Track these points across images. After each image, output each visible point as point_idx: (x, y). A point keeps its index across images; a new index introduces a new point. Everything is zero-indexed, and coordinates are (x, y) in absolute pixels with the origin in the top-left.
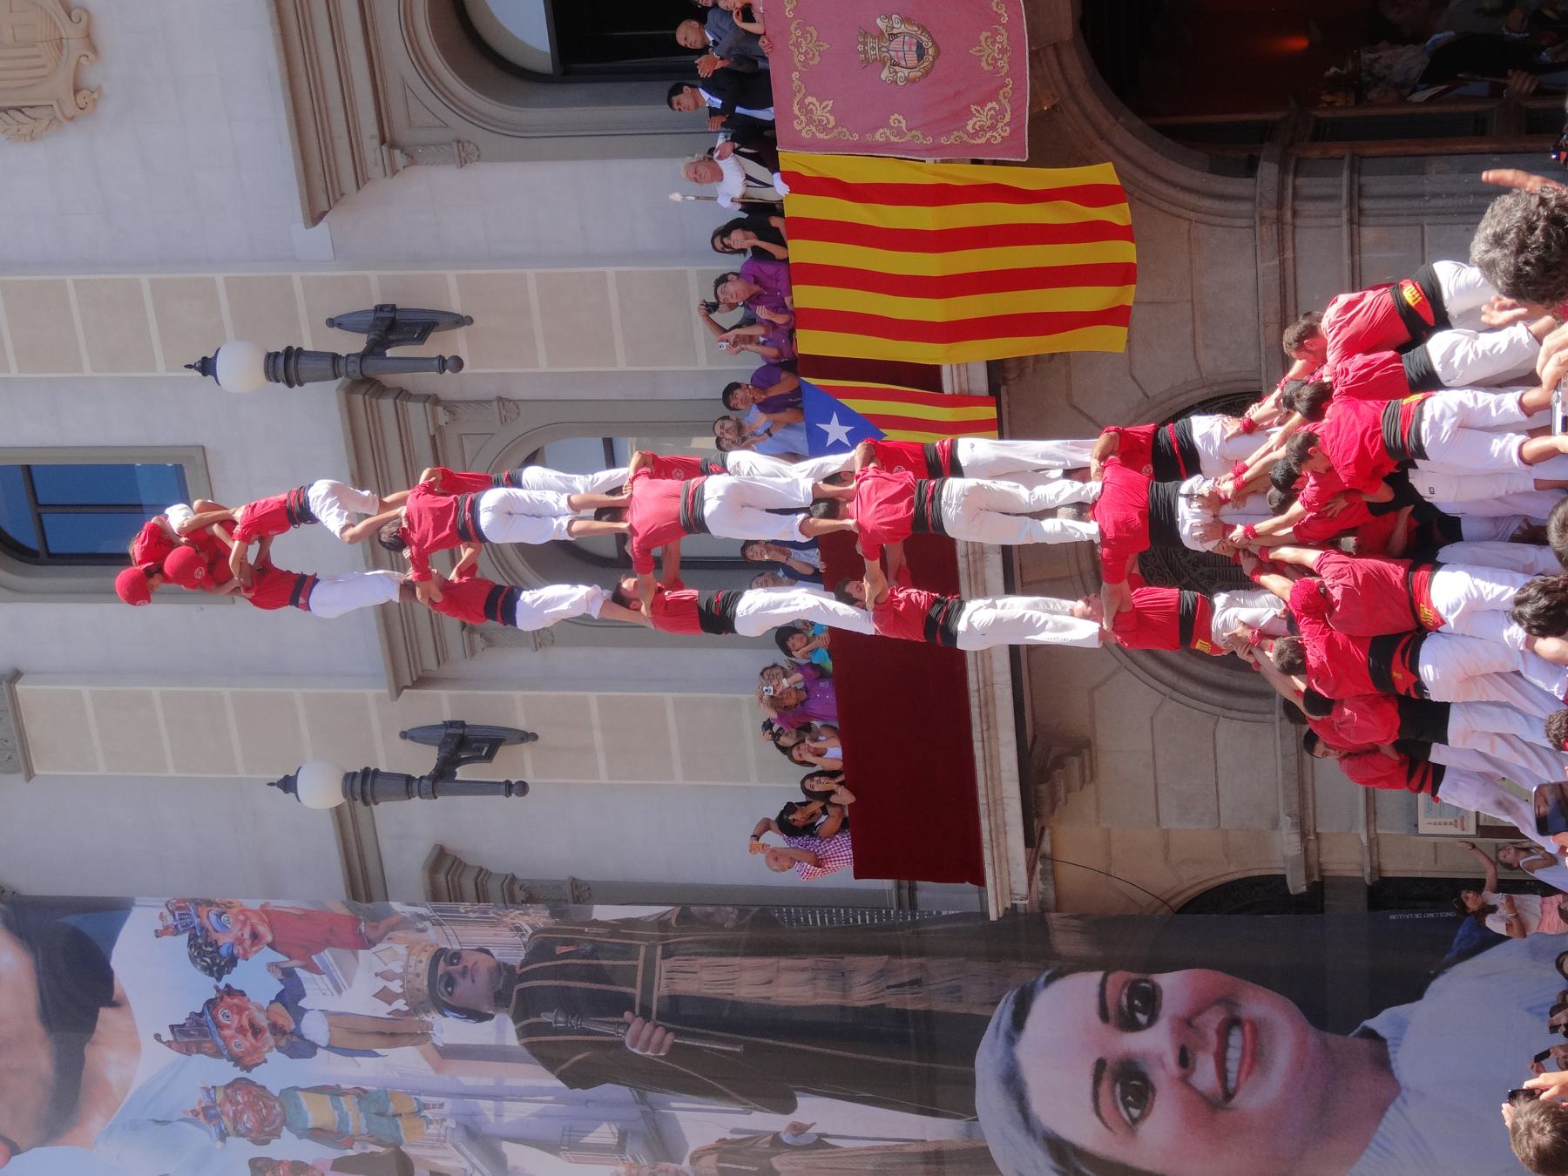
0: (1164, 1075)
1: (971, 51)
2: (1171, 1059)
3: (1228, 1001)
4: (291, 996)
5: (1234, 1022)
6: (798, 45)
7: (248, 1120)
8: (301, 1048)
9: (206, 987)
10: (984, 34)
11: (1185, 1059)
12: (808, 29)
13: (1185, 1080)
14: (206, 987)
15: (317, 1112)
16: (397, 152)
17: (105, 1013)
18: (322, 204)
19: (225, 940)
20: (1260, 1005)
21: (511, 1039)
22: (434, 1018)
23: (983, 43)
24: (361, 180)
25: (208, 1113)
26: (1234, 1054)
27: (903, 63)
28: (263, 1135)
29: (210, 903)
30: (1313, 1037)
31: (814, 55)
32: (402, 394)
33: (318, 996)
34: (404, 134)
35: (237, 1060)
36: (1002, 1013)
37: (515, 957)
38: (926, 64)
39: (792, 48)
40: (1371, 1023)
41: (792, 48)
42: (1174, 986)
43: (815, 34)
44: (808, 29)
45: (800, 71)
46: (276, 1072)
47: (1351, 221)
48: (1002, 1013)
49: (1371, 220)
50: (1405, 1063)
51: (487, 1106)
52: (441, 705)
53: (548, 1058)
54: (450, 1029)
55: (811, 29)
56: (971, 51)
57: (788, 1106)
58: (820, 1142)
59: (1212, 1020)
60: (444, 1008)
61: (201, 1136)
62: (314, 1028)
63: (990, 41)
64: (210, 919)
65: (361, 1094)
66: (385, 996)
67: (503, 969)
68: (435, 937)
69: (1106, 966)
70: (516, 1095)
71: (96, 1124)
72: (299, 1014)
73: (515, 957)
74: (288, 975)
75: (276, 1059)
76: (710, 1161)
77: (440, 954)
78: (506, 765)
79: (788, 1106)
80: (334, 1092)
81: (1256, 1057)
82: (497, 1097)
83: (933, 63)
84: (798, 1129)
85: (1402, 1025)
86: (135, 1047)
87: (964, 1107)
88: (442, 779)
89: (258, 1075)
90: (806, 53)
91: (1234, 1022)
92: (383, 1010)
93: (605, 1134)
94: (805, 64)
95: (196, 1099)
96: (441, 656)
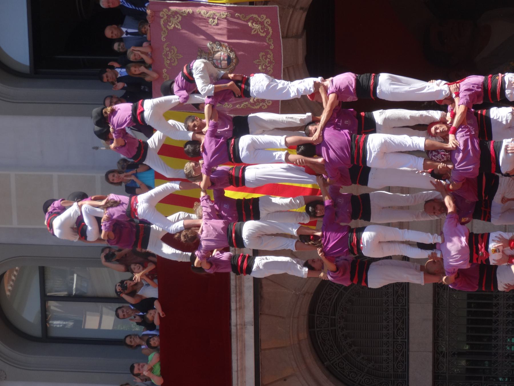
1: (254, 62)
6: (167, 55)
10: (261, 54)
12: (172, 47)
23: (261, 58)
27: (220, 66)
31: (174, 60)
38: (231, 67)
39: (163, 56)
41: (163, 56)
43: (176, 50)
44: (172, 47)
45: (167, 69)
55: (174, 47)
56: (254, 62)
63: (264, 57)
83: (235, 67)
90: (170, 60)
94: (170, 65)
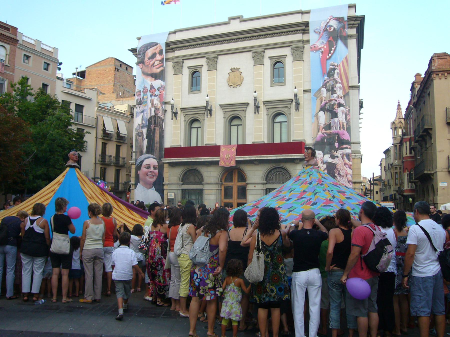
0: (149, 170)
2: (151, 171)
3: (155, 176)
4: (156, 96)
5: (153, 176)
7: (144, 91)
8: (151, 96)
9: (156, 88)
11: (150, 172)
13: (149, 172)
14: (156, 88)
15: (145, 97)
17: (154, 79)
19: (160, 90)
20: (155, 178)
21: (152, 115)
22: (154, 108)
25: (145, 87)
26: (151, 176)
28: (143, 92)
29: (164, 89)
30: (152, 182)
32: (205, 111)
33: (156, 98)
35: (150, 90)
36: (154, 157)
37: (159, 115)
40: (153, 187)
42: (157, 171)
46: (149, 94)
48: (154, 157)
50: (150, 190)
51: (146, 112)
52: (179, 112)
53: (151, 118)
54: (153, 110)
57: (146, 138)
58: (143, 141)
59: (154, 174)
60: (155, 109)
61: (143, 86)
62: (153, 97)
64: (162, 88)
65: (147, 101)
66: (156, 104)
67: (158, 114)
68: (161, 108)
69: (158, 166)
70: (147, 115)
71: (144, 77)
72: (154, 96)
73: (159, 115)
74: (157, 95)
75: (150, 94)
76: (141, 131)
77: (159, 109)
78: (174, 119)
79: (146, 138)
80: (147, 99)
81: (151, 178)
82: (147, 113)
84: (144, 139)
85: (153, 190)
86: (151, 81)
87: (146, 154)
88: (173, 112)
89: (148, 92)
91: (153, 176)
92: (155, 104)
93: (144, 122)
95: (146, 86)
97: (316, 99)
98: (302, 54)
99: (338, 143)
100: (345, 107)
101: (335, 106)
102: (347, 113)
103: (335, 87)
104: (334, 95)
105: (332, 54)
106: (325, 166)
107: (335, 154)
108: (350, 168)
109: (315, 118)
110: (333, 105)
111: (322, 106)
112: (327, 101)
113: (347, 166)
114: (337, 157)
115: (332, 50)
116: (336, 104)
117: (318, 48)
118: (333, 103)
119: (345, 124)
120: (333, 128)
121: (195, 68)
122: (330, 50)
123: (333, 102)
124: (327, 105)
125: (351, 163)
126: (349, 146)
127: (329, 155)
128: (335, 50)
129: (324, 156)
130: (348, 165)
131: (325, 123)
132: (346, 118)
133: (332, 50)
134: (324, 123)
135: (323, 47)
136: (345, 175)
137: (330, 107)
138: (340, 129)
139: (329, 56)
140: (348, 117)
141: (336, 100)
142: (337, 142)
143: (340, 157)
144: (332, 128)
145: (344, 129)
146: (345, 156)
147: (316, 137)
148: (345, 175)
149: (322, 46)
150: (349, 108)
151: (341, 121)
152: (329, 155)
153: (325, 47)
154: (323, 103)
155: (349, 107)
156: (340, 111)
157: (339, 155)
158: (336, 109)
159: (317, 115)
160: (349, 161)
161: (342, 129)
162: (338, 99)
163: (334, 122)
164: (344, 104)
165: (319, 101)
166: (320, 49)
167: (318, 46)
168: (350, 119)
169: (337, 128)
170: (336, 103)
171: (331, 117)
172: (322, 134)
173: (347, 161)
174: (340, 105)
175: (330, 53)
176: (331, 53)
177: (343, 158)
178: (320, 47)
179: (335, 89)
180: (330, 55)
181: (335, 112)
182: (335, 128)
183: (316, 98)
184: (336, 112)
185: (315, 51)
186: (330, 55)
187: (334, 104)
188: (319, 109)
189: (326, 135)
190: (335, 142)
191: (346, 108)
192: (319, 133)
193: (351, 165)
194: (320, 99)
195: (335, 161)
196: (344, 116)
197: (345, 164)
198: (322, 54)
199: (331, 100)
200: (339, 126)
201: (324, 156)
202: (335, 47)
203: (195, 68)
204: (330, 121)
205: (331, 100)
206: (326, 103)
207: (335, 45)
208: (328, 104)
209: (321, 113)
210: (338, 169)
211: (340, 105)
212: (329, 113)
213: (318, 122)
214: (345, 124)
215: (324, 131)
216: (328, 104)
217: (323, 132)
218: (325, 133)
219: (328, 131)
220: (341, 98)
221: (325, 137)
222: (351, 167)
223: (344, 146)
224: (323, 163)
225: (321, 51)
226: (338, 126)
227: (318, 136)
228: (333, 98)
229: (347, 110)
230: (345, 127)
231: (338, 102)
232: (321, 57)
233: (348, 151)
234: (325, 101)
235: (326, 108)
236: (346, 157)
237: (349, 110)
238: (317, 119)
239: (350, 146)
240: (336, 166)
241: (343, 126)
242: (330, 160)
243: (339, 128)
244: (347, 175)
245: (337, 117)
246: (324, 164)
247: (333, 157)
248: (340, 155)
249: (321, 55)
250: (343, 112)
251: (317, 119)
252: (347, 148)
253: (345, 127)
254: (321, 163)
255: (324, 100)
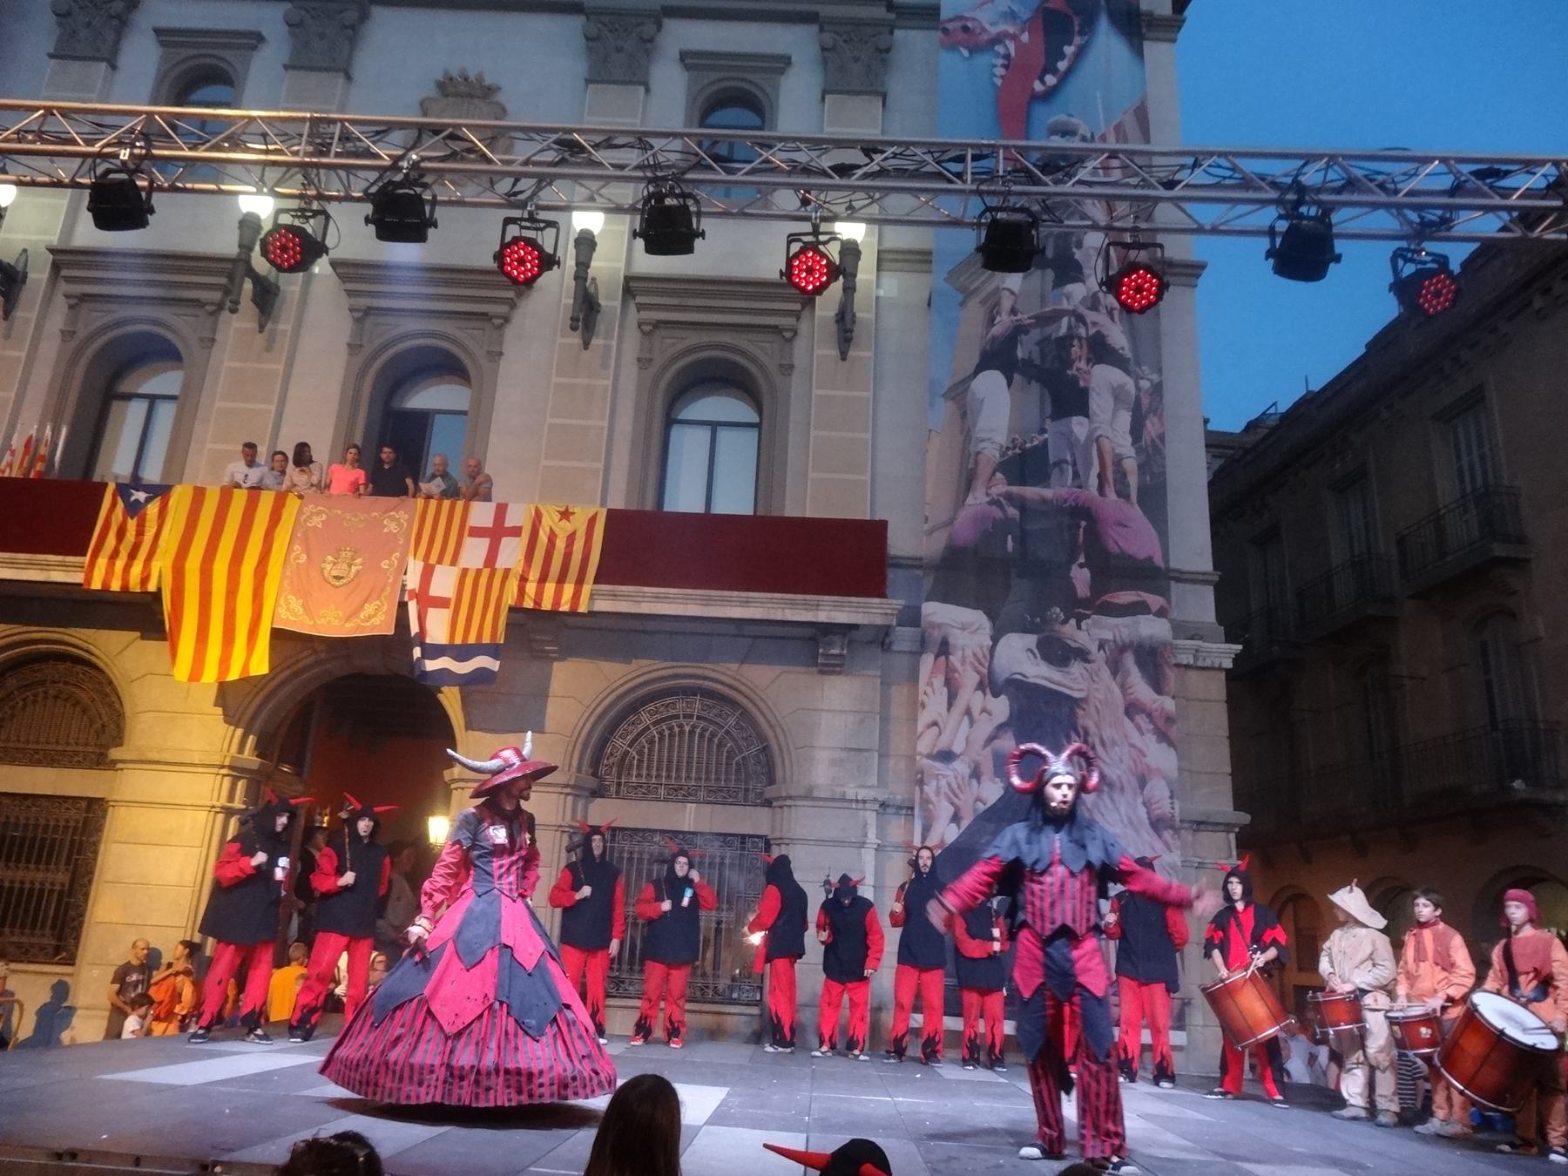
16: (361, 314)
18: (340, 270)
24: (350, 293)
34: (370, 320)
47: (213, 807)
49: (211, 818)
96: (69, 280)
97: (962, 304)
98: (884, 61)
99: (1086, 572)
100: (1132, 367)
101: (1075, 350)
102: (1145, 402)
103: (1079, 245)
104: (1070, 288)
105: (1065, 77)
106: (1001, 707)
107: (1070, 632)
108: (1163, 736)
109: (945, 409)
110: (1065, 342)
111: (994, 338)
112: (1024, 317)
113: (1141, 720)
114: (1082, 655)
115: (1062, 56)
116: (1080, 339)
117: (985, 37)
118: (1063, 330)
119: (1130, 465)
120: (1062, 472)
121: (203, 45)
122: (1055, 54)
123: (1064, 325)
124: (1024, 337)
125: (1169, 704)
126: (1155, 601)
127: (1031, 640)
128: (1081, 53)
129: (995, 639)
130: (1149, 715)
131: (1013, 440)
132: (1136, 431)
133: (1062, 56)
134: (1002, 438)
135: (1014, 37)
136: (1131, 782)
137: (1043, 357)
138: (1101, 489)
139: (1043, 82)
140: (1151, 428)
141: (1081, 319)
142: (1082, 560)
143: (1099, 657)
144: (1055, 474)
145: (1123, 494)
146: (1129, 660)
147: (951, 522)
148: (1134, 783)
149: (1011, 29)
150: (1155, 377)
151: (1106, 444)
152: (1031, 640)
153: (1025, 37)
154: (1004, 322)
155: (1160, 371)
156: (1102, 379)
157: (1093, 647)
158: (1082, 365)
159: (959, 393)
160: (1159, 690)
161: (1112, 495)
162: (1091, 316)
163: (1071, 442)
164: (1128, 353)
165: (975, 312)
166: (998, 39)
167: (984, 30)
168: (1162, 437)
169: (1088, 477)
170: (1082, 331)
171: (1049, 410)
172: (991, 503)
173: (1142, 690)
174: (1100, 351)
175: (1050, 68)
176: (1054, 71)
177: (1115, 667)
178: (994, 30)
179: (1078, 255)
180: (1051, 80)
181: (1075, 379)
182: (1076, 475)
183: (960, 297)
184: (1082, 383)
185: (965, 53)
186: (1051, 80)
187: (1069, 338)
188: (976, 360)
189: (1013, 512)
190: (1072, 559)
191: (1137, 378)
192: (970, 500)
193: (1169, 720)
194: (983, 302)
195: (1071, 680)
196: (1125, 418)
197: (1133, 709)
198: (1006, 67)
199: (1056, 316)
200: (1095, 470)
201: (995, 639)
202: (1078, 40)
203: (203, 45)
204: (1043, 431)
205: (1056, 316)
206: (1019, 330)
207: (1081, 33)
208: (1036, 334)
209: (991, 384)
210: (1087, 733)
211: (1100, 351)
212: (1035, 386)
213: (967, 435)
214: (1130, 465)
215: (1001, 487)
216: (1036, 334)
217: (995, 491)
218: (1009, 497)
219: (1030, 492)
220: (1110, 313)
221: (1008, 520)
222: (1174, 732)
223: (1126, 597)
224: (991, 684)
225: (1000, 49)
226: (1089, 465)
227: (964, 515)
228: (1065, 305)
229: (1145, 384)
230: (1133, 481)
231: (1092, 331)
232: (999, 82)
233: (1152, 628)
234: (1013, 311)
235: (1020, 353)
236: (1140, 664)
237: (1157, 389)
238: (964, 415)
239: (1164, 593)
240: (1073, 715)
241: (1121, 475)
242: (1038, 672)
243: (1093, 482)
244: (1143, 782)
245: (1086, 415)
246: (996, 695)
247: (1057, 653)
248: (1101, 647)
249: (1001, 71)
250: (1118, 394)
251: (964, 415)
252: (1139, 608)
253: (1133, 481)
254: (980, 686)
255: (1007, 303)
